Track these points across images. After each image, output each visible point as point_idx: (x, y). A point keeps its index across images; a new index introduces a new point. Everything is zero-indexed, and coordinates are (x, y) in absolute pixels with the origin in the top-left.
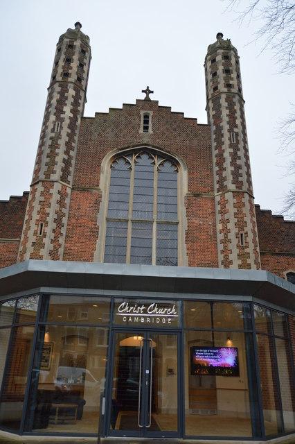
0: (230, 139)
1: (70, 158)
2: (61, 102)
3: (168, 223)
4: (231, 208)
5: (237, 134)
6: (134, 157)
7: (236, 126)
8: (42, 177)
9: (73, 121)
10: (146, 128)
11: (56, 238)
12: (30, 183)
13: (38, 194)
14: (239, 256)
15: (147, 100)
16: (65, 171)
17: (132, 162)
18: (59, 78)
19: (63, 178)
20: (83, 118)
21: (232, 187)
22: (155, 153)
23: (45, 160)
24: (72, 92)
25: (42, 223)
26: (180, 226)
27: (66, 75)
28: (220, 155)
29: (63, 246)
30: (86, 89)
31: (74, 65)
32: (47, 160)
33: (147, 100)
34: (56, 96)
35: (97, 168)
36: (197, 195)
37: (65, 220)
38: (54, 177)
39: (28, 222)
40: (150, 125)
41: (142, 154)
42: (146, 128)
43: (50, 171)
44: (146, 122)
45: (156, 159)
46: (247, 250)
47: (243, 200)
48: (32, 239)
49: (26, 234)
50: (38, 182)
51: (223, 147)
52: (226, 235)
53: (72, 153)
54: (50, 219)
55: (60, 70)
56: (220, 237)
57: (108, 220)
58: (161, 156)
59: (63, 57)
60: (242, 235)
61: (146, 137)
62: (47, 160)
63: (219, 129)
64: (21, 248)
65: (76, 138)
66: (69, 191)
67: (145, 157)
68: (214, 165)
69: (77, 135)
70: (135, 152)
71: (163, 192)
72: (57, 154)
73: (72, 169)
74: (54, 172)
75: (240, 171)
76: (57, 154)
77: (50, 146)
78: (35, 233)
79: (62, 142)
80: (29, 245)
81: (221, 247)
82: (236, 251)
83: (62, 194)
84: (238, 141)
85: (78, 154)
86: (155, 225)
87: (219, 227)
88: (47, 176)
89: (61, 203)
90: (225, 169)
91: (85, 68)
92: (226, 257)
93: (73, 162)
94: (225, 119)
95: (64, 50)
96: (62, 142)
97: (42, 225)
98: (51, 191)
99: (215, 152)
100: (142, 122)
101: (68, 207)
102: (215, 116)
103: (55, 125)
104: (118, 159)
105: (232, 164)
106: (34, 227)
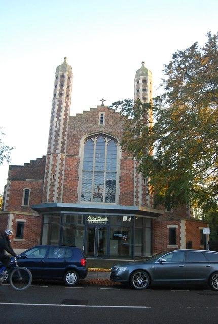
1: (65, 140)
2: (59, 111)
3: (112, 173)
6: (96, 138)
8: (52, 151)
9: (66, 120)
10: (102, 121)
11: (60, 181)
15: (103, 105)
16: (63, 148)
18: (58, 96)
19: (62, 152)
20: (70, 117)
23: (53, 143)
26: (117, 173)
27: (61, 94)
31: (65, 88)
33: (103, 105)
34: (57, 107)
35: (77, 145)
37: (63, 172)
39: (47, 173)
40: (104, 120)
42: (102, 121)
43: (56, 149)
44: (102, 118)
45: (106, 139)
48: (50, 182)
53: (66, 138)
54: (57, 173)
55: (58, 92)
56: (135, 180)
57: (83, 171)
58: (109, 137)
59: (59, 83)
61: (102, 127)
64: (44, 186)
65: (67, 129)
66: (65, 157)
67: (101, 138)
71: (110, 157)
72: (58, 139)
73: (65, 146)
78: (51, 179)
79: (60, 133)
80: (48, 185)
81: (135, 185)
83: (62, 160)
86: (105, 173)
88: (55, 151)
89: (61, 164)
91: (70, 87)
93: (66, 142)
95: (59, 79)
98: (57, 159)
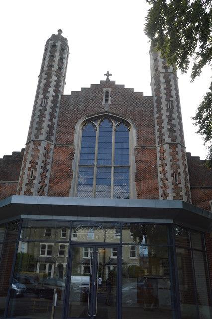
0: (167, 105)
1: (53, 124)
2: (47, 85)
3: (123, 168)
4: (167, 154)
5: (172, 102)
7: (171, 96)
8: (33, 137)
9: (55, 98)
10: (107, 100)
12: (26, 143)
13: (30, 150)
14: (174, 190)
15: (108, 80)
16: (50, 133)
17: (97, 125)
19: (48, 138)
20: (63, 96)
21: (168, 140)
22: (113, 117)
23: (35, 125)
24: (54, 78)
25: (33, 169)
28: (160, 117)
29: (47, 186)
30: (65, 75)
31: (57, 59)
32: (37, 126)
33: (108, 80)
34: (44, 81)
36: (143, 147)
37: (49, 167)
38: (42, 137)
39: (23, 169)
41: (104, 119)
42: (107, 100)
46: (180, 186)
47: (177, 149)
48: (26, 181)
49: (22, 177)
50: (30, 142)
51: (162, 112)
52: (164, 175)
53: (55, 120)
54: (38, 167)
56: (160, 176)
58: (117, 119)
60: (176, 174)
61: (107, 107)
62: (37, 126)
63: (159, 98)
64: (19, 188)
65: (57, 110)
66: (52, 147)
67: (106, 121)
68: (156, 124)
69: (58, 107)
70: (99, 117)
72: (44, 121)
74: (41, 134)
75: (175, 129)
76: (44, 121)
77: (39, 116)
78: (28, 177)
79: (47, 113)
80: (24, 185)
81: (160, 184)
82: (171, 187)
83: (47, 149)
84: (172, 107)
85: (59, 120)
87: (160, 169)
90: (163, 127)
91: (64, 61)
92: (165, 191)
93: (55, 126)
94: (163, 91)
96: (47, 113)
97: (33, 171)
99: (156, 115)
100: (104, 96)
101: (51, 158)
102: (157, 91)
103: (42, 101)
104: (87, 123)
105: (169, 123)
106: (27, 173)
